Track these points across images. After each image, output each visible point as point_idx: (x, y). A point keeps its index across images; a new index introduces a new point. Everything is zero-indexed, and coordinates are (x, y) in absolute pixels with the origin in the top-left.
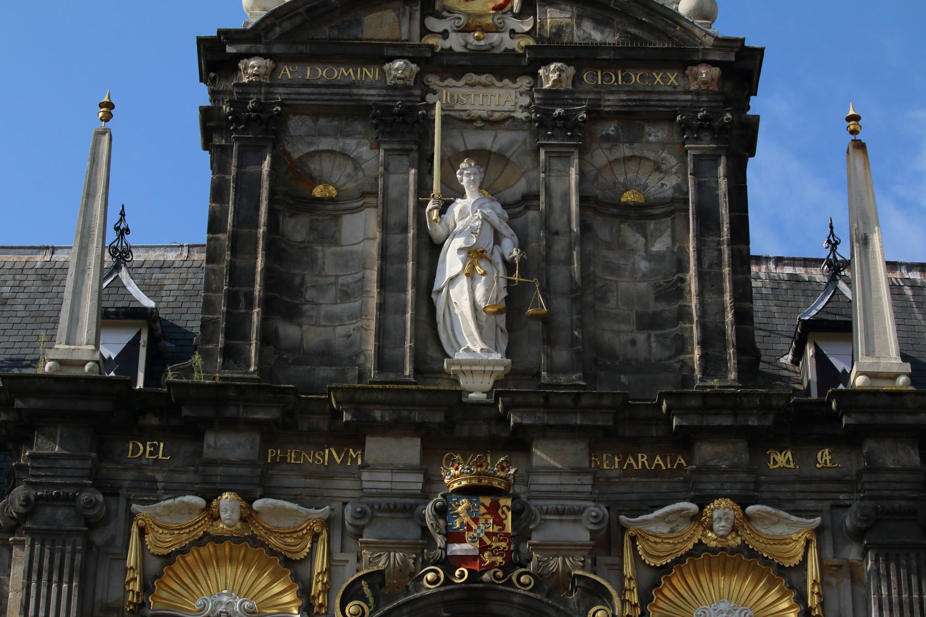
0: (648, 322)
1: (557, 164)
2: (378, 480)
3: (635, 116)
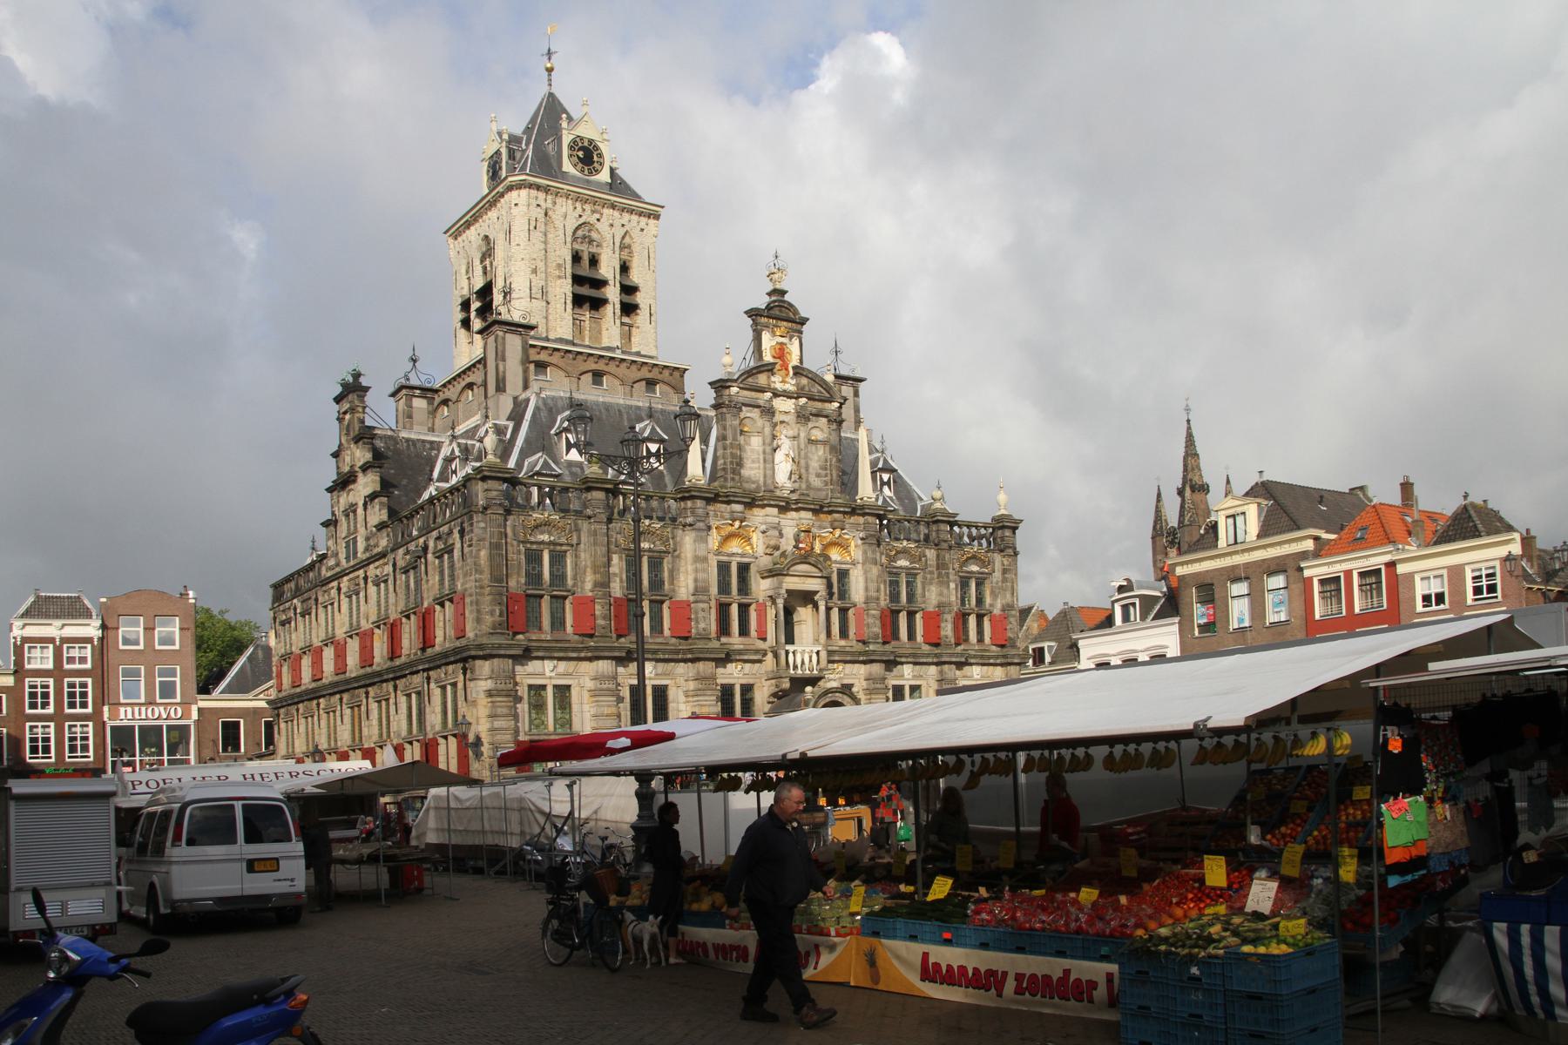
0: (818, 475)
2: (770, 519)
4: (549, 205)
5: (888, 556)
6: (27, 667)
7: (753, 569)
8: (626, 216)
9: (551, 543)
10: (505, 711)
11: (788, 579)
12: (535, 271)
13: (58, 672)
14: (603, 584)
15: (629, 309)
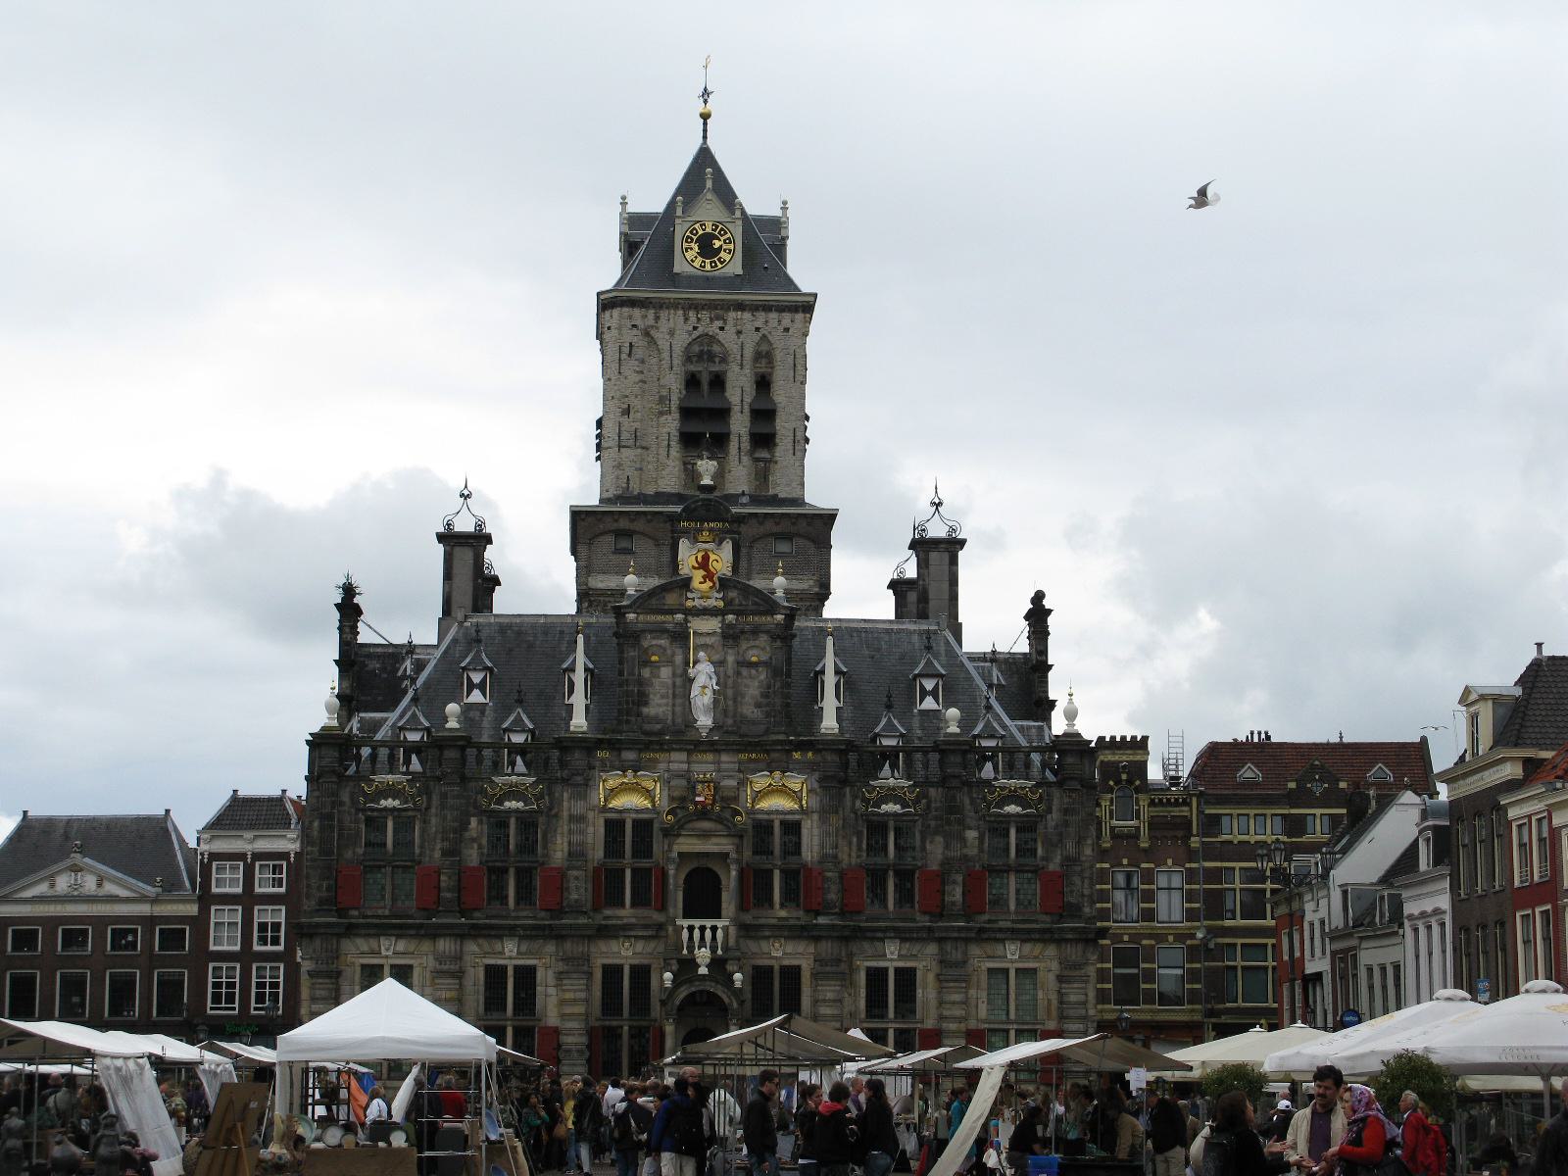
0: (758, 705)
1: (730, 651)
2: (674, 766)
3: (756, 632)
4: (650, 321)
5: (866, 801)
6: (215, 890)
7: (656, 826)
8: (761, 316)
9: (394, 809)
10: (323, 993)
11: (681, 840)
12: (627, 412)
13: (248, 899)
14: (452, 852)
15: (763, 440)
